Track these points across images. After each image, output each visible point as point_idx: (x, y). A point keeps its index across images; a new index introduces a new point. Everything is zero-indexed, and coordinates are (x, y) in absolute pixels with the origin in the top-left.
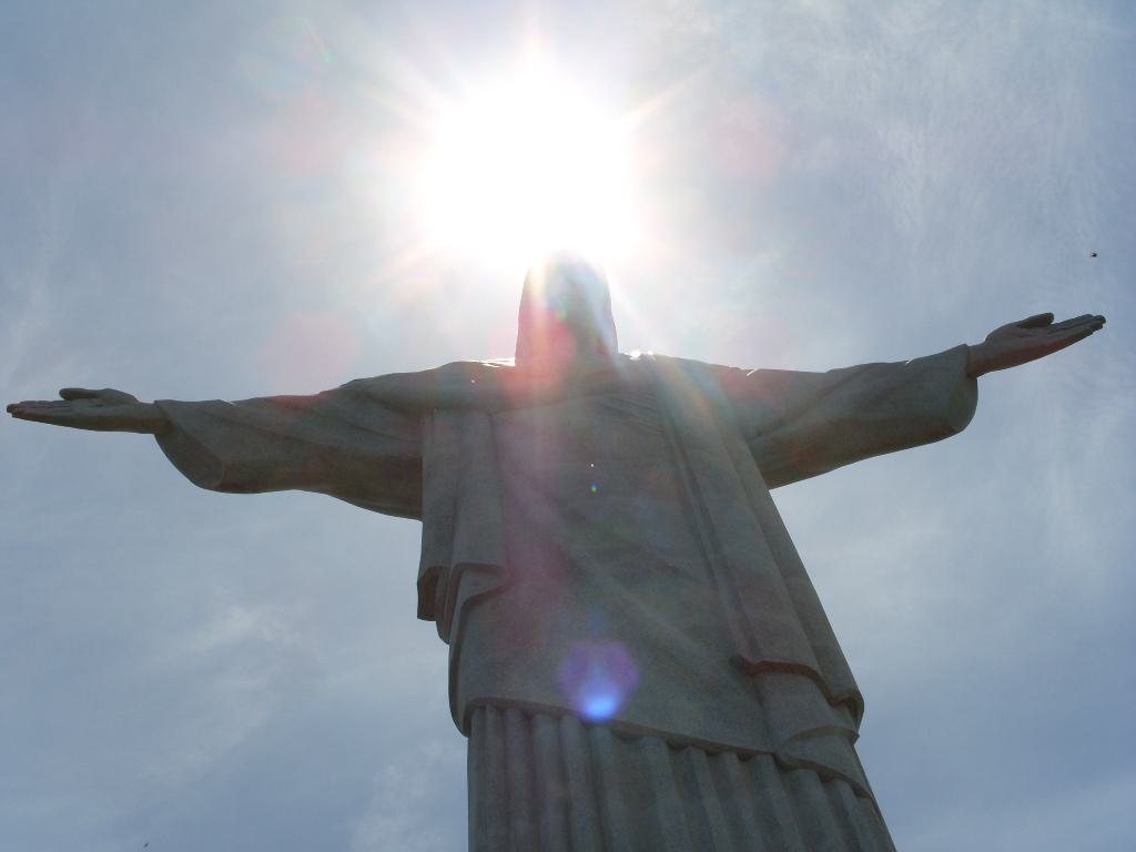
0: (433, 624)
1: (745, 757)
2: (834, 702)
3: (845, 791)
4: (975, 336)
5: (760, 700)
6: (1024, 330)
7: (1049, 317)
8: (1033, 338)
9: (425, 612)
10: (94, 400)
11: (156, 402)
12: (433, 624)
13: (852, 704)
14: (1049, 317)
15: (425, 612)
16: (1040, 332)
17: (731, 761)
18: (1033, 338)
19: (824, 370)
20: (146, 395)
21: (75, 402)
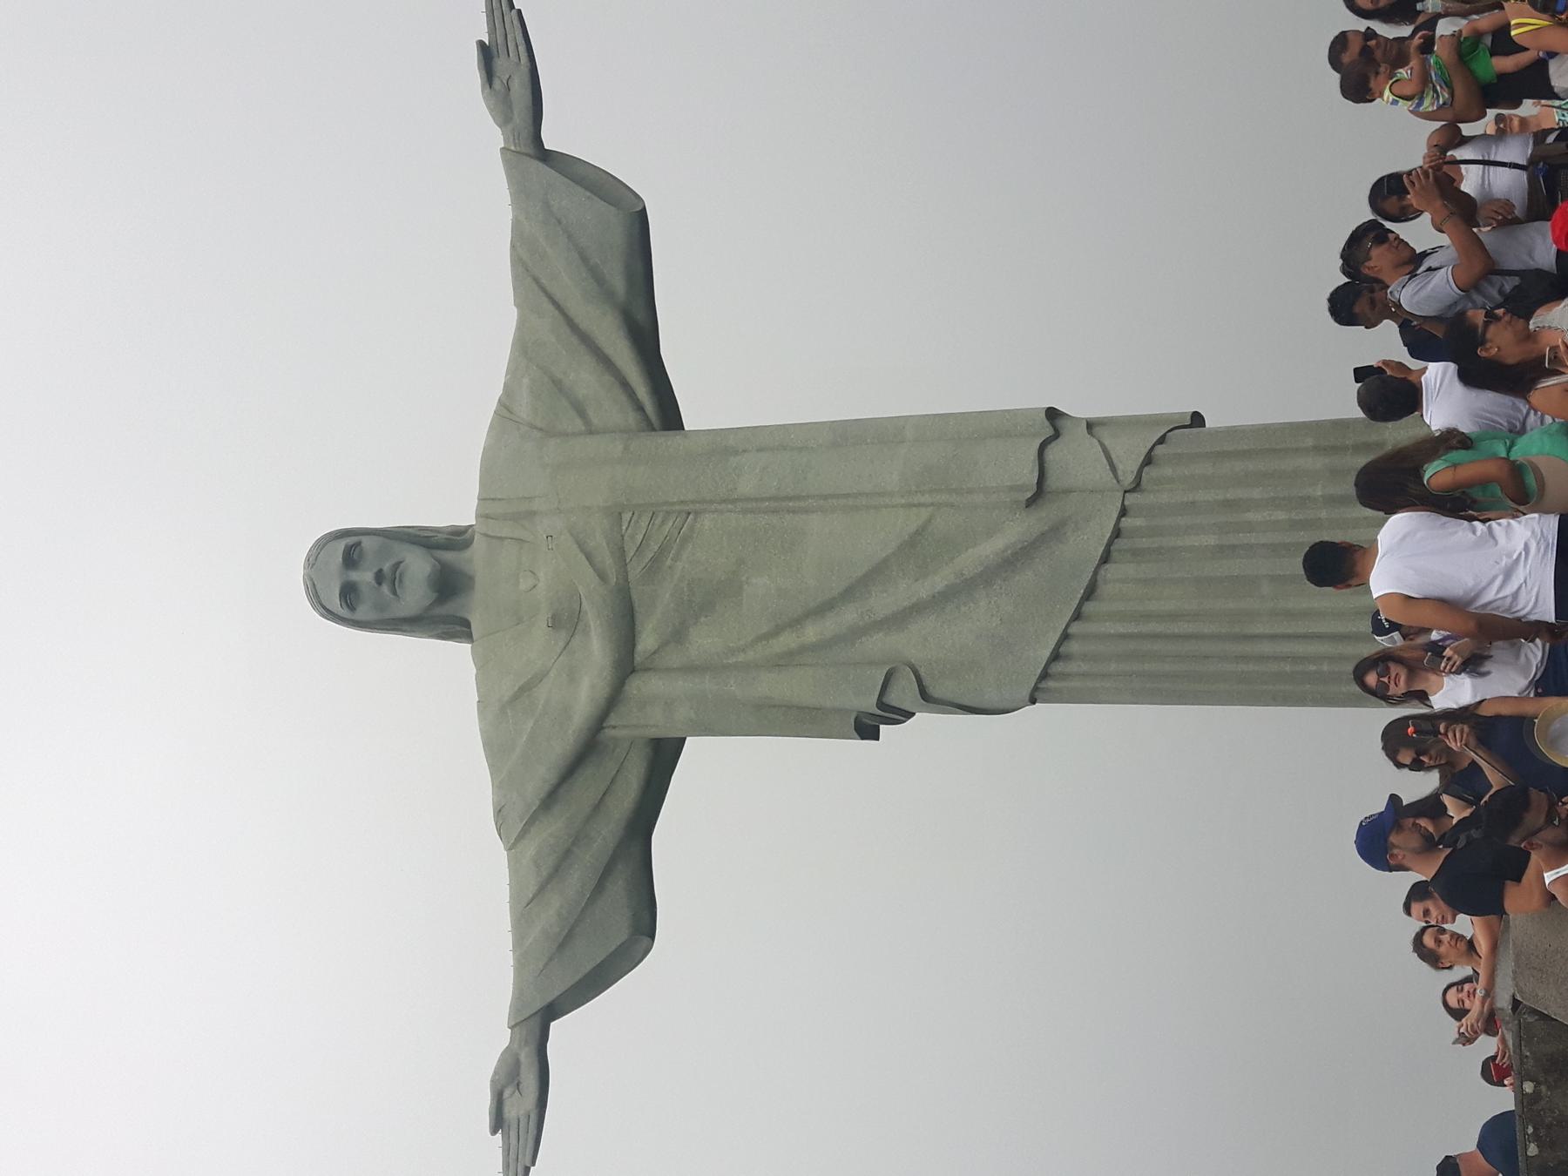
0: (882, 727)
1: (1123, 512)
2: (1057, 435)
3: (1160, 449)
4: (494, 137)
5: (1068, 491)
6: (497, 84)
7: (481, 44)
8: (509, 69)
9: (875, 735)
10: (506, 1094)
11: (512, 1028)
12: (882, 727)
13: (1053, 414)
14: (481, 44)
15: (875, 735)
16: (500, 64)
17: (1126, 522)
18: (509, 69)
19: (512, 315)
20: (502, 1038)
21: (511, 1112)
